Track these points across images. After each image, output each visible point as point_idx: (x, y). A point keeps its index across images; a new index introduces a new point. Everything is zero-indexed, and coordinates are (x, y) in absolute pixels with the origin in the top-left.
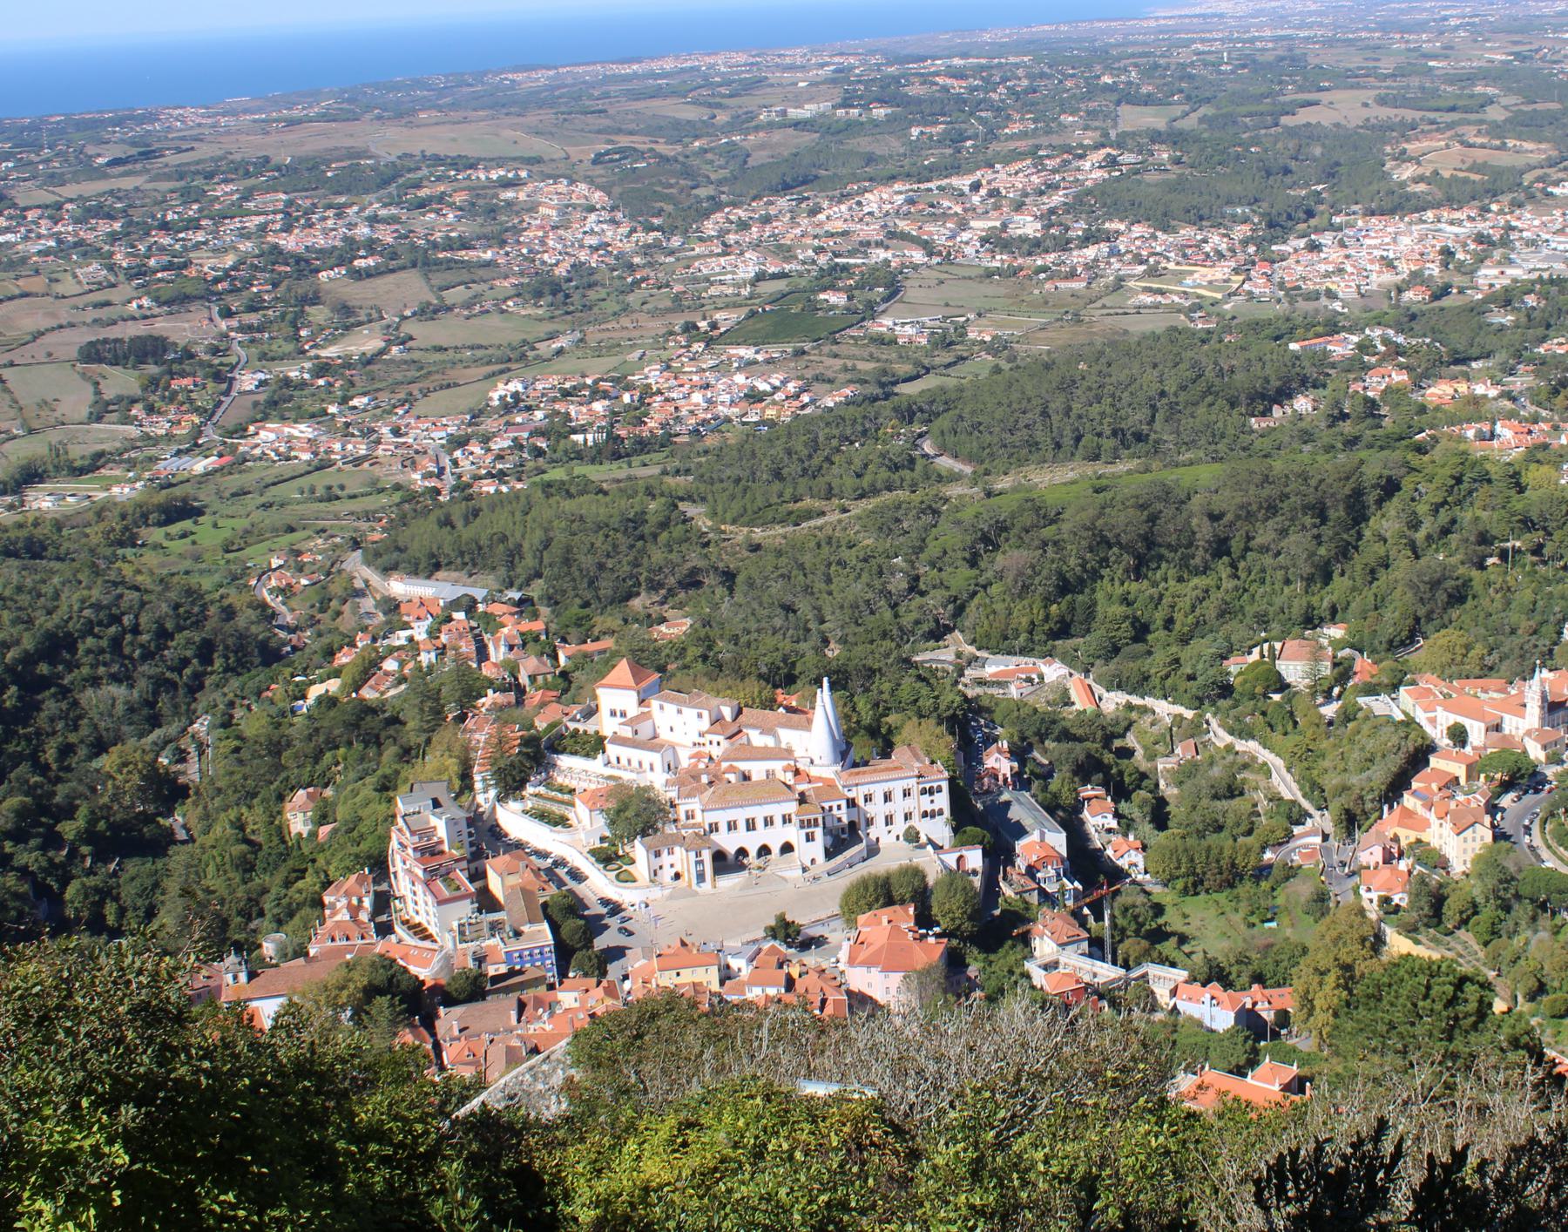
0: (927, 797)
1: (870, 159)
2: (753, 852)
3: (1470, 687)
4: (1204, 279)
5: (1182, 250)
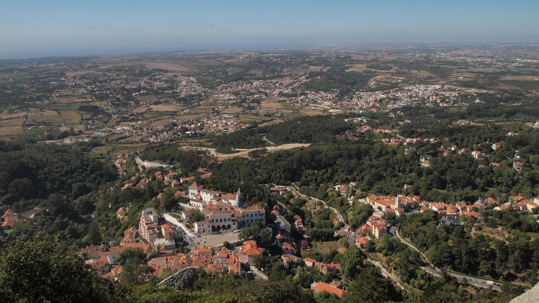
0: (260, 217)
1: (254, 75)
3: (381, 197)
4: (326, 104)
5: (322, 98)
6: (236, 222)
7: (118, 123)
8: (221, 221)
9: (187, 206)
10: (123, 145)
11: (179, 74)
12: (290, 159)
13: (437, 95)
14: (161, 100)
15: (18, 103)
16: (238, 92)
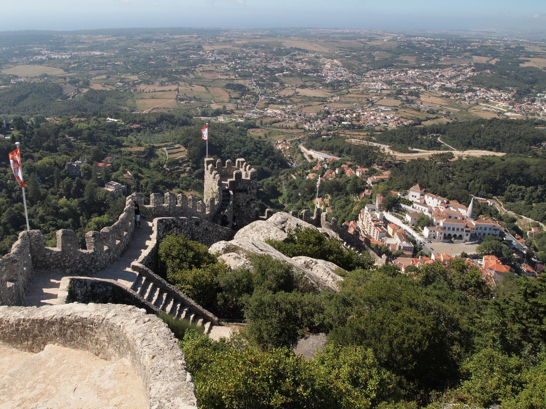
1: (406, 62)
4: (501, 106)
5: (495, 97)
6: (469, 234)
7: (267, 105)
8: (453, 229)
9: (409, 208)
10: (277, 129)
11: (320, 56)
12: (491, 168)
14: (307, 84)
15: (167, 76)
16: (391, 81)
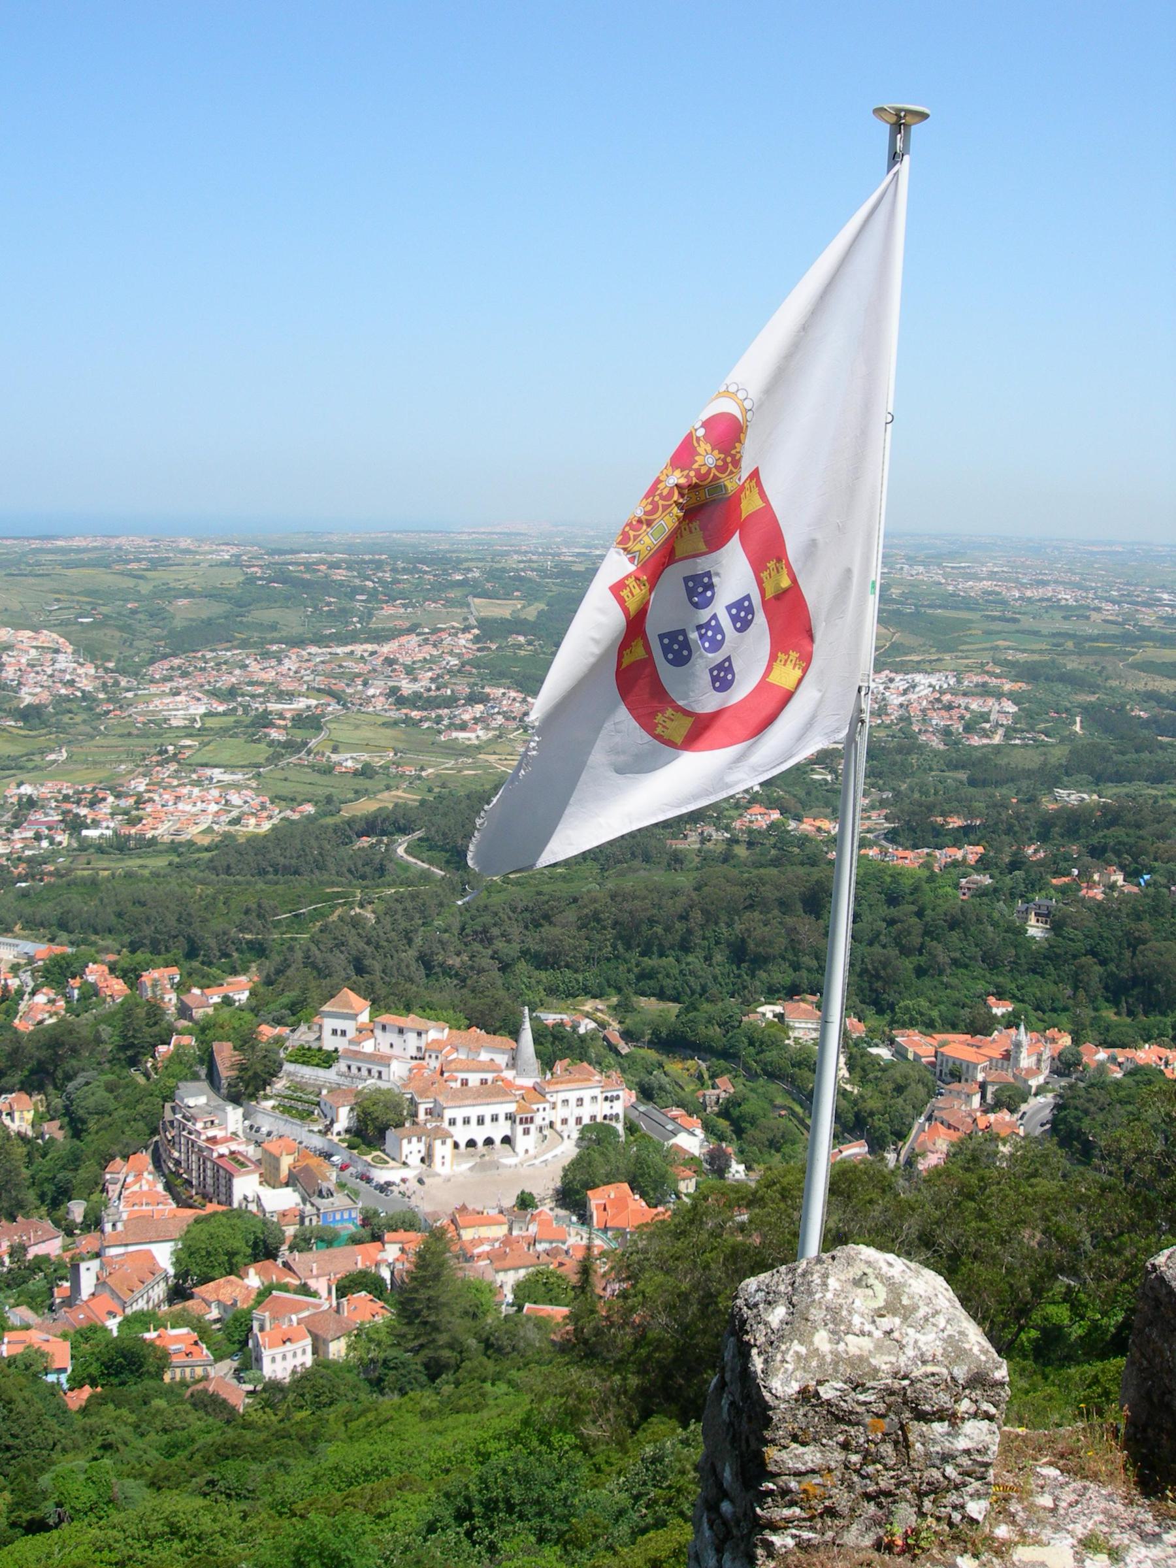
0: (608, 1104)
1: (273, 627)
2: (480, 1143)
6: (532, 1127)
8: (481, 1121)
13: (949, 707)
